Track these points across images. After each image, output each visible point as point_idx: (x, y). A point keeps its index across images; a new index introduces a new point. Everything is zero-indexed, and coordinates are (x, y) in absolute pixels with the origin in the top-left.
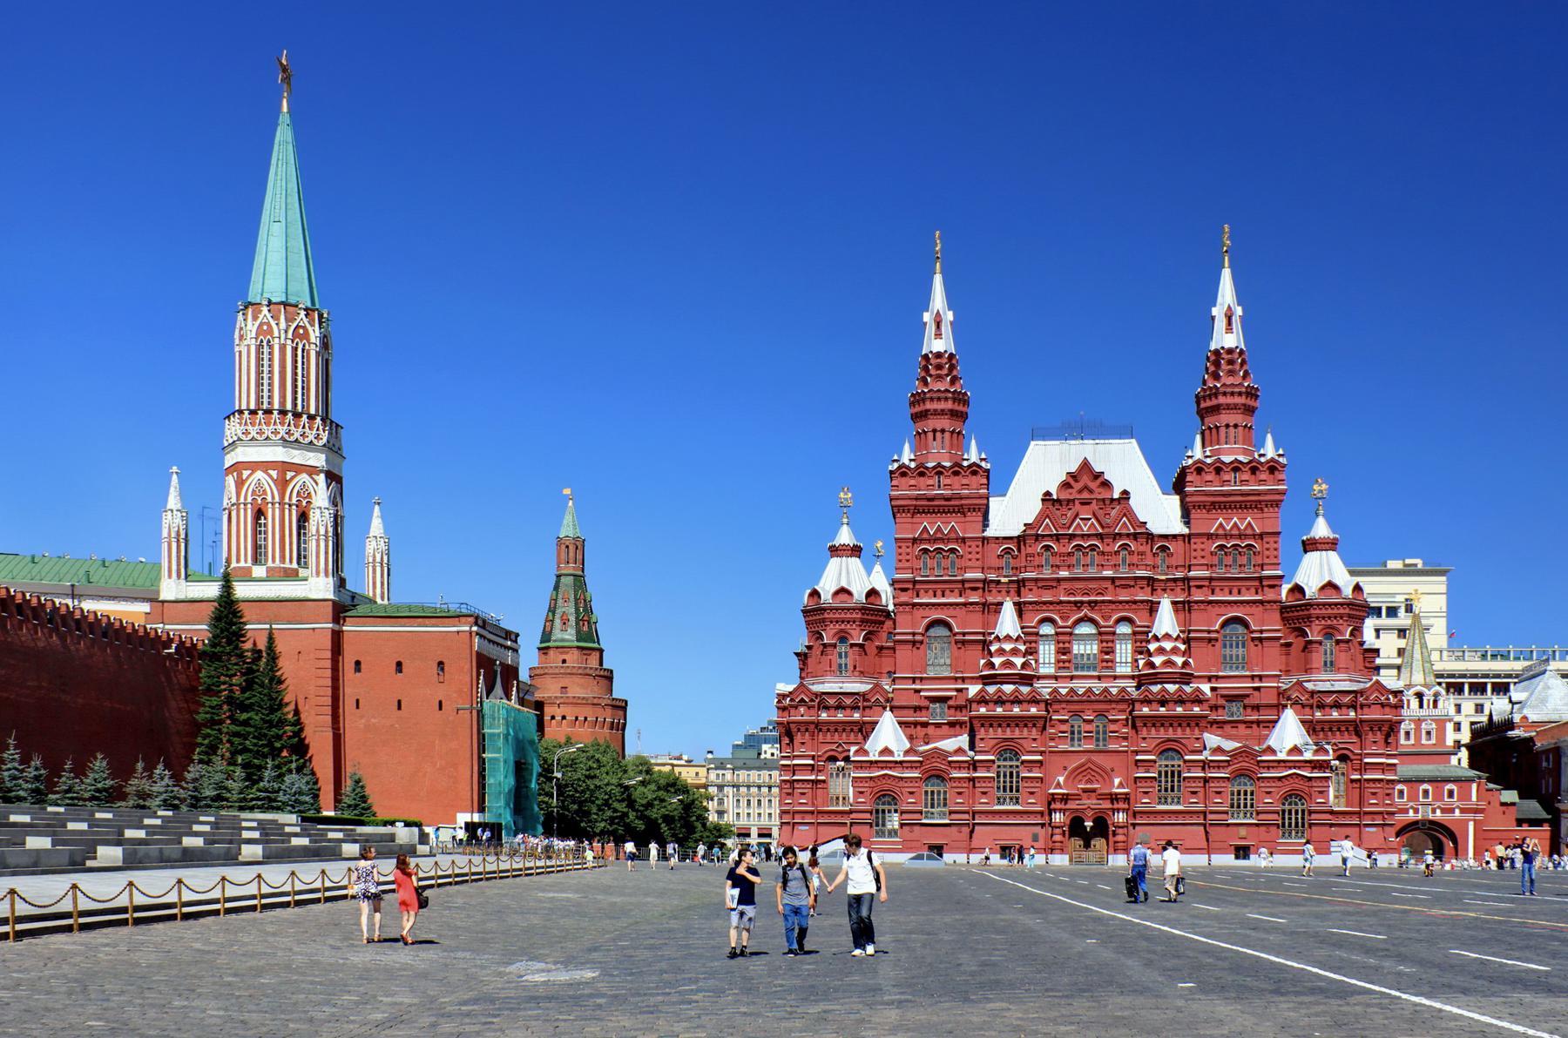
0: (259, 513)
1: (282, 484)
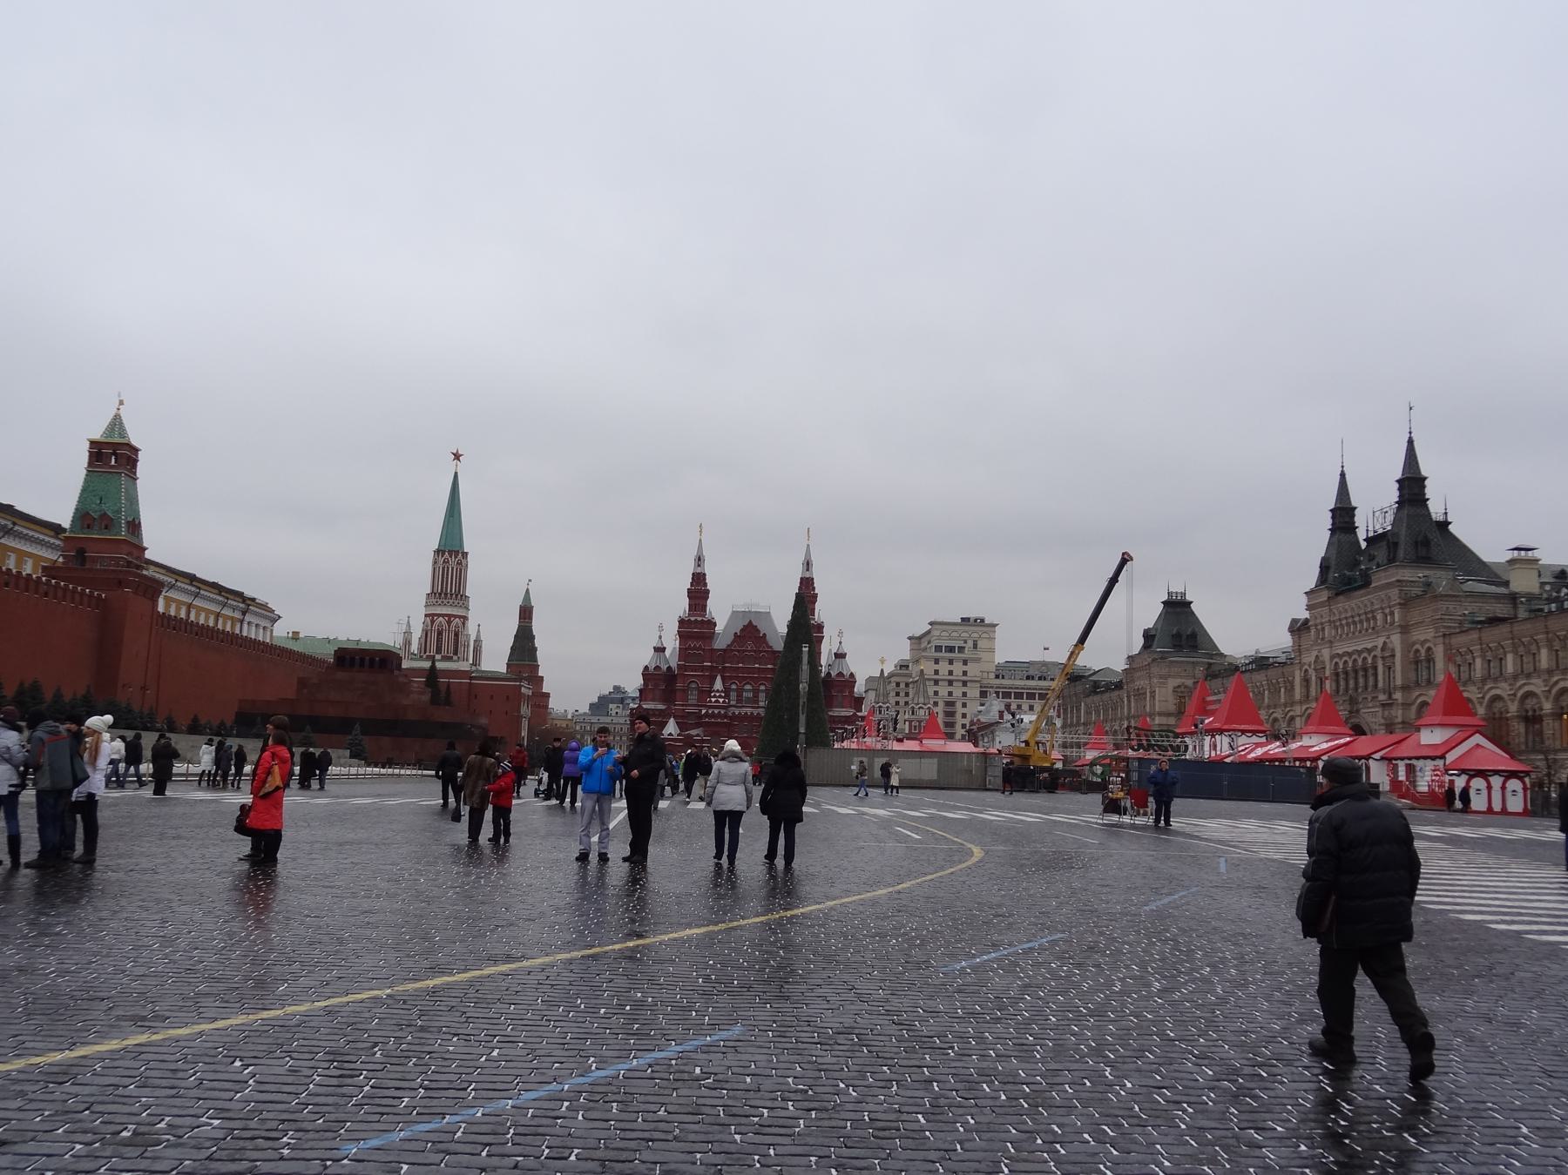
0: (440, 633)
1: (449, 623)
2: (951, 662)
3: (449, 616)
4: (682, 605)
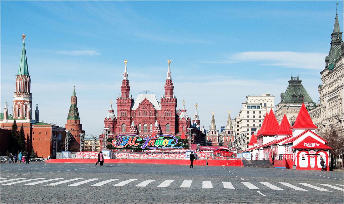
2: (254, 112)
4: (119, 94)
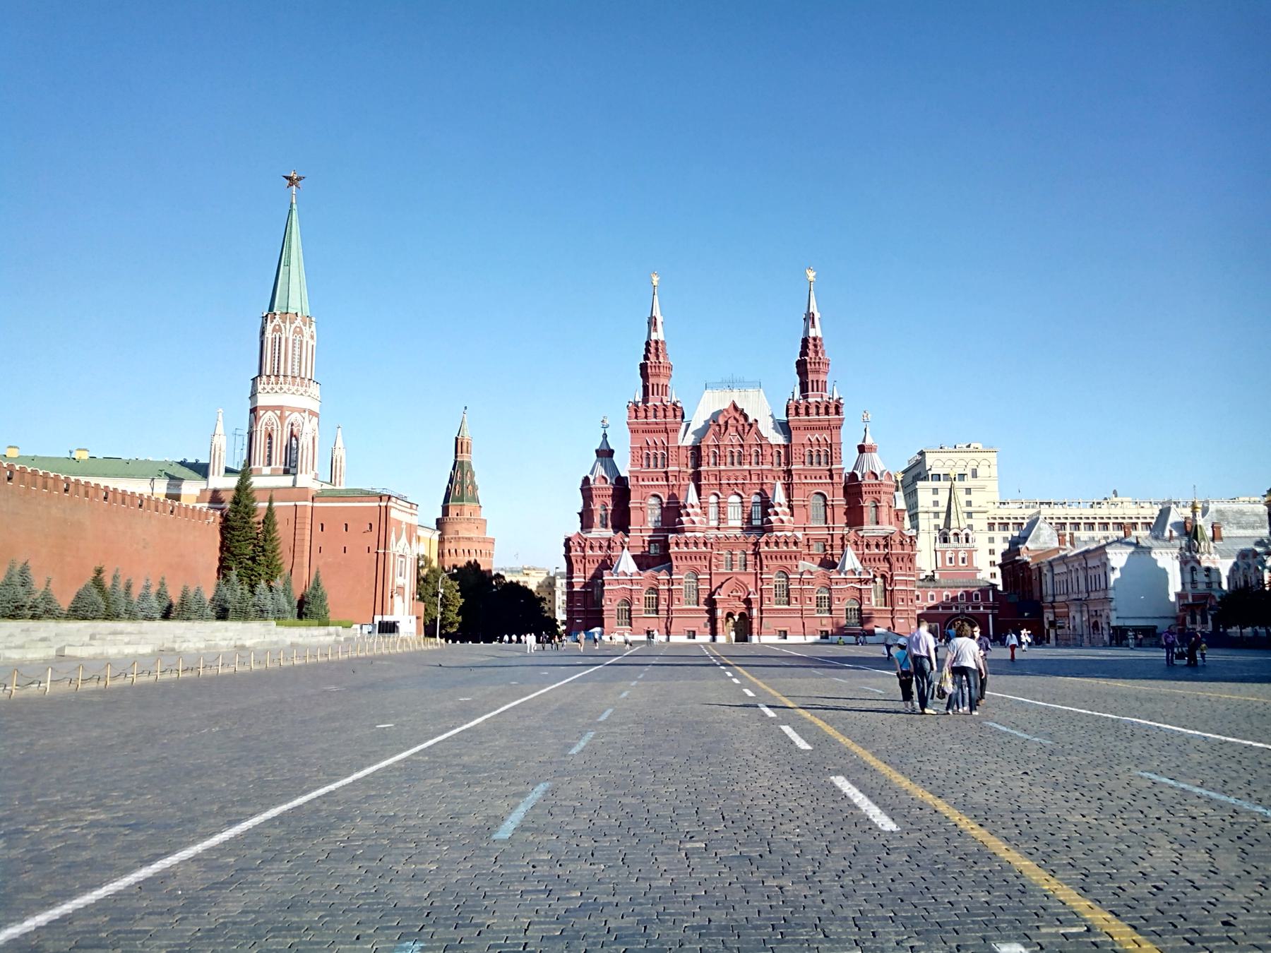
3: (280, 408)
